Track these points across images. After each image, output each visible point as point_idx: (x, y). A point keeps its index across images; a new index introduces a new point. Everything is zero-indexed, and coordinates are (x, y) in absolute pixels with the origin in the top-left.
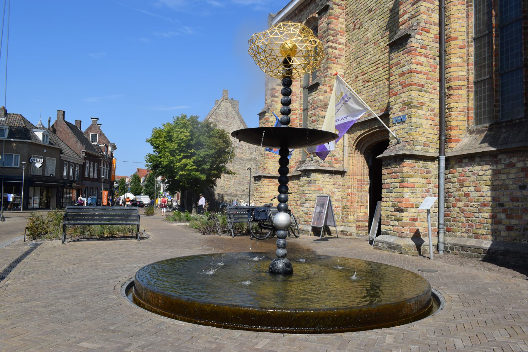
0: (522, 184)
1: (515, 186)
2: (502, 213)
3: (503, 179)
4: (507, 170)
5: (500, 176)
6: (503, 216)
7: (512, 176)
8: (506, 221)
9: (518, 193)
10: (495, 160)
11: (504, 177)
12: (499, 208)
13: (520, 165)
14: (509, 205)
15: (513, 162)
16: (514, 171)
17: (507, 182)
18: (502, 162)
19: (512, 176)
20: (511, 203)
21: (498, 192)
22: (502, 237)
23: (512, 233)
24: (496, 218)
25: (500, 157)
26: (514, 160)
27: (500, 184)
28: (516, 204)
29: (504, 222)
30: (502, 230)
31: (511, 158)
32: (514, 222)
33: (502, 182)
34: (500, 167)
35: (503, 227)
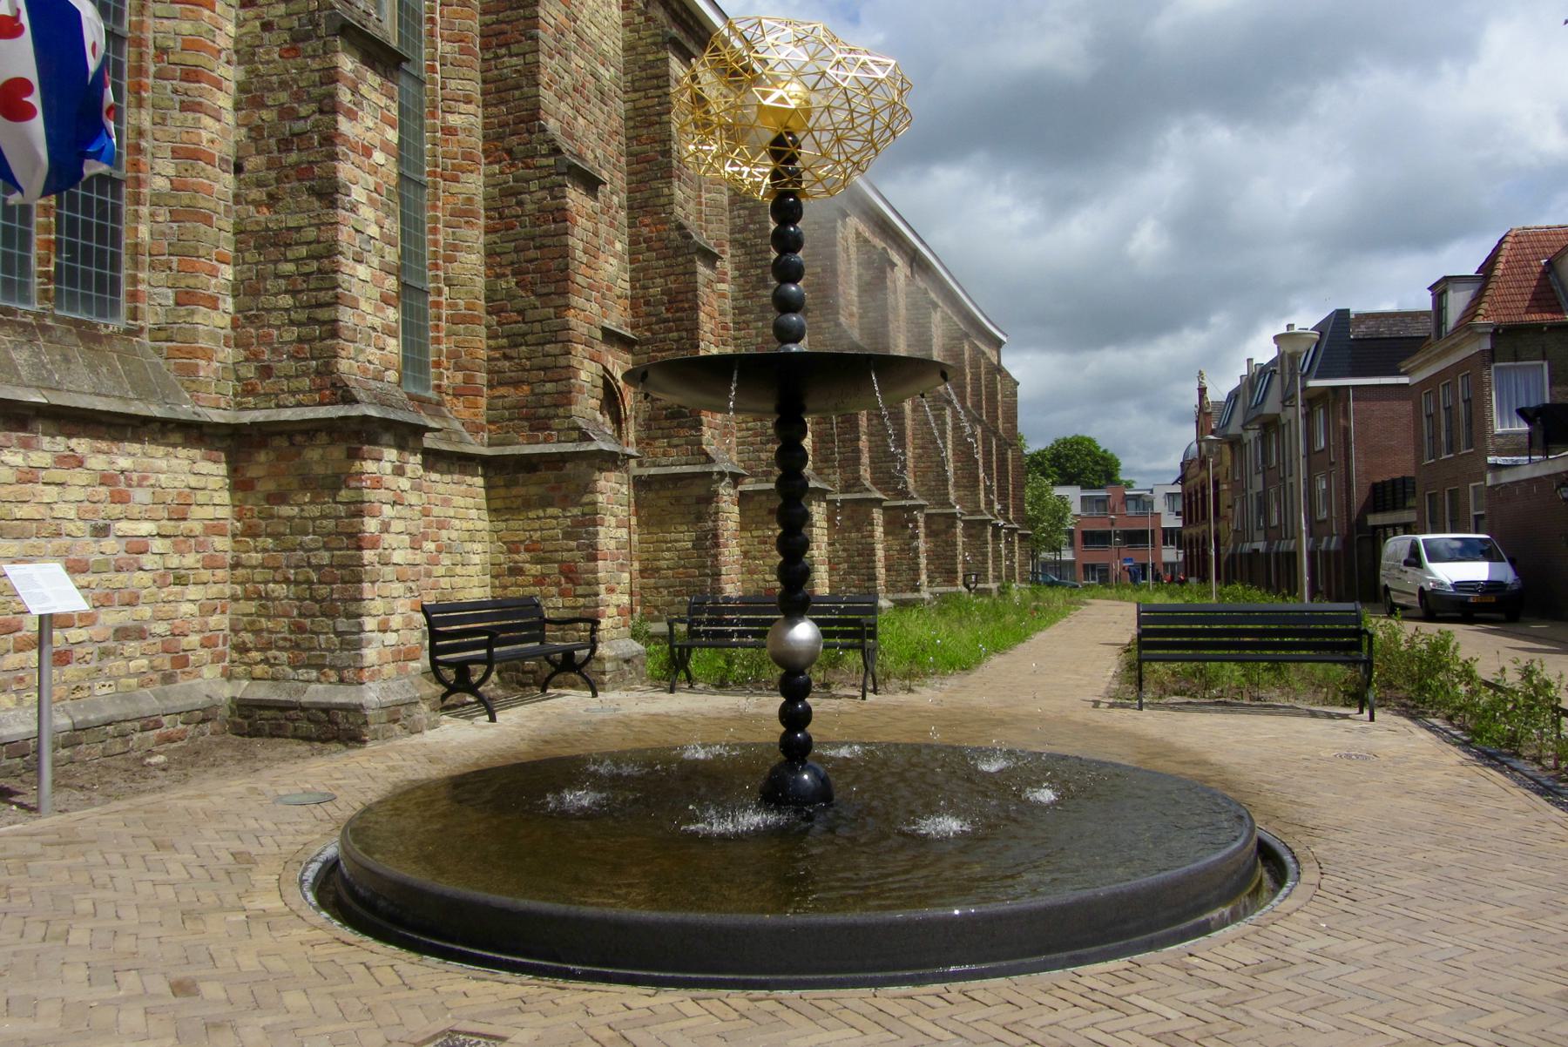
0: (101, 523)
1: (80, 523)
4: (58, 475)
7: (75, 493)
11: (51, 493)
13: (97, 463)
16: (78, 477)
17: (62, 510)
19: (75, 493)
24: (19, 630)
26: (81, 445)
33: (43, 509)
34: (37, 458)
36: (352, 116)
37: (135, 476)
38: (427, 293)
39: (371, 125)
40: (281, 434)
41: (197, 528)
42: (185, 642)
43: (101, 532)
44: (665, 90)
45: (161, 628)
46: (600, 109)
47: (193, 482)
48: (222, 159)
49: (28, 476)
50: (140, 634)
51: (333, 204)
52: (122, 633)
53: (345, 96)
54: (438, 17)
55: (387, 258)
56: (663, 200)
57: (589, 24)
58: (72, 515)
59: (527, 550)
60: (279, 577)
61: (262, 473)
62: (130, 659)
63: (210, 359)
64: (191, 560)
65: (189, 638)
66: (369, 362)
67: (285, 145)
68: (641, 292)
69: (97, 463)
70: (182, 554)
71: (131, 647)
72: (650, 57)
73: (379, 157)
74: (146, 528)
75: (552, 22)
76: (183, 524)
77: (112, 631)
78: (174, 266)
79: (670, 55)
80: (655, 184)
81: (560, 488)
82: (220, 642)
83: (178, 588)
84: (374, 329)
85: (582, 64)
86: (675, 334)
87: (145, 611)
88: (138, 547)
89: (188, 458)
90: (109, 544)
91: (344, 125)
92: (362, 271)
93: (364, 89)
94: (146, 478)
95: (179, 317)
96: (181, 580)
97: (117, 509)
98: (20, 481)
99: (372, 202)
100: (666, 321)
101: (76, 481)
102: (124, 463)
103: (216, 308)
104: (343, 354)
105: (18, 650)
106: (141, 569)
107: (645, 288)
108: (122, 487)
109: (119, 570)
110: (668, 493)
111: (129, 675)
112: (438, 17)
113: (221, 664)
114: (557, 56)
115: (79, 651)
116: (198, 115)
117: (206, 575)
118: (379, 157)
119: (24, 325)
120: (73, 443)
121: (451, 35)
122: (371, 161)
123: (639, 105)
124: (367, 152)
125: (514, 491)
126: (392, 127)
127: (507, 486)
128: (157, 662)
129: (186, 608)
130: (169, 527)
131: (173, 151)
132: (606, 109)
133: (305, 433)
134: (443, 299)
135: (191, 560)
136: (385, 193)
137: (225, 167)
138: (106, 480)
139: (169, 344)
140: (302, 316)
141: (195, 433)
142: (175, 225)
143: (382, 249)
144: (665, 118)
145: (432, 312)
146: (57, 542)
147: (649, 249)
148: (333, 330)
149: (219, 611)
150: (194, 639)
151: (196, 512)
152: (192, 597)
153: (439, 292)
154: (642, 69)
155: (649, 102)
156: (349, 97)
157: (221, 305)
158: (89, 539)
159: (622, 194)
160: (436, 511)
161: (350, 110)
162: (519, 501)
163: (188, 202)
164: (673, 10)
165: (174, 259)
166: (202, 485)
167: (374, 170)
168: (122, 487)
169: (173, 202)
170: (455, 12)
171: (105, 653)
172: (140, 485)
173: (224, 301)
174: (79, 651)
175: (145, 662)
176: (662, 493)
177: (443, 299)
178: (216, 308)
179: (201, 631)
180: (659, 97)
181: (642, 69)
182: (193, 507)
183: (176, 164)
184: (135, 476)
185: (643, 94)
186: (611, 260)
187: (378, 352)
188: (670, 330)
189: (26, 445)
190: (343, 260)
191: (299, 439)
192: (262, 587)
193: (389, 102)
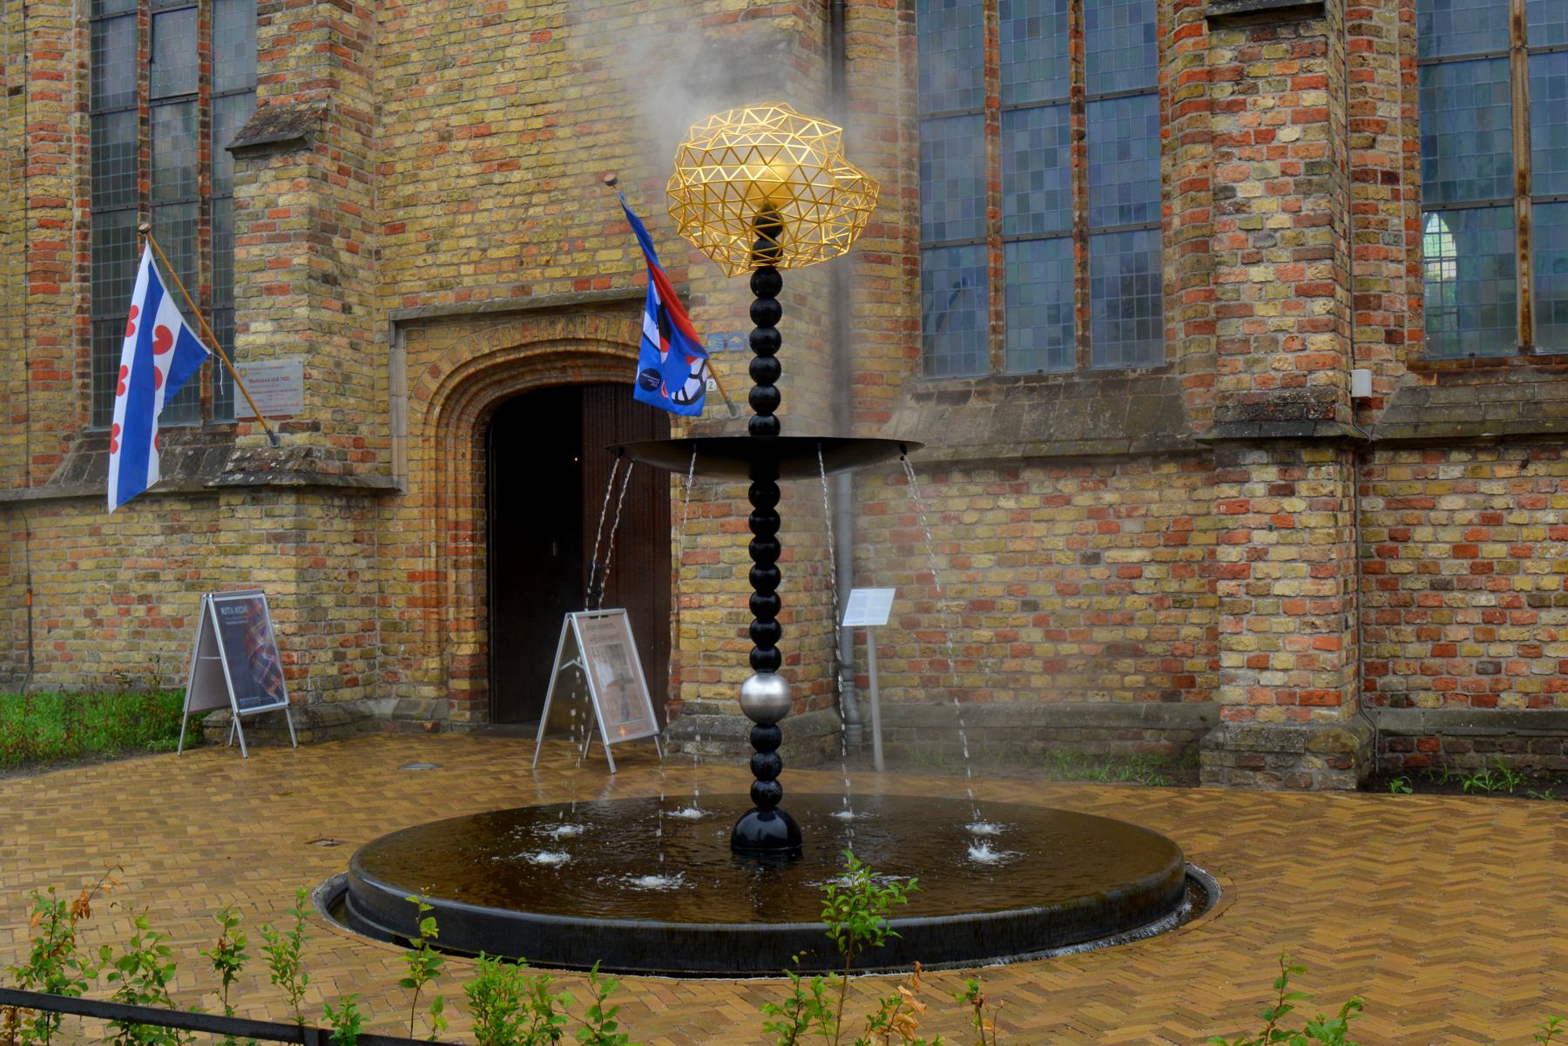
0: (1089, 552)
2: (1034, 625)
3: (1036, 534)
4: (1047, 512)
5: (1028, 525)
6: (1036, 635)
7: (1062, 528)
8: (1047, 649)
9: (1081, 575)
10: (1013, 483)
11: (1040, 530)
12: (1025, 614)
13: (1084, 500)
14: (1052, 602)
15: (1066, 491)
16: (1067, 514)
17: (1050, 543)
18: (1035, 489)
19: (1062, 528)
20: (1059, 600)
21: (1021, 569)
22: (1032, 690)
23: (1062, 680)
24: (1015, 640)
25: (1027, 475)
26: (1068, 486)
27: (1028, 548)
28: (1071, 602)
29: (1038, 650)
30: (1033, 673)
31: (1058, 479)
32: (1066, 648)
33: (1033, 543)
34: (1027, 501)
35: (1038, 664)
37: (1123, 510)
42: (1188, 665)
43: (1092, 559)
45: (1158, 648)
47: (1191, 509)
49: (1021, 516)
50: (1136, 651)
52: (1116, 650)
58: (1061, 545)
62: (1126, 674)
69: (1084, 500)
70: (1182, 579)
71: (1126, 663)
73: (1287, 134)
74: (1137, 555)
76: (1181, 551)
77: (1102, 647)
83: (1179, 612)
87: (1142, 633)
88: (1132, 573)
89: (1185, 486)
90: (1098, 572)
94: (1135, 509)
96: (1179, 603)
97: (1105, 539)
98: (1013, 521)
101: (1063, 517)
102: (1109, 497)
105: (1014, 657)
106: (1134, 593)
108: (1112, 519)
109: (1110, 593)
111: (1123, 688)
115: (1071, 663)
119: (1050, 388)
120: (1061, 485)
124: (1266, 136)
128: (1156, 679)
129: (1186, 631)
130: (1164, 553)
138: (1093, 513)
141: (1193, 461)
146: (1047, 570)
151: (1197, 538)
158: (1079, 566)
166: (1203, 510)
168: (1112, 519)
171: (1098, 666)
172: (1129, 516)
174: (1071, 663)
175: (1140, 678)
184: (1123, 510)
189: (1018, 491)
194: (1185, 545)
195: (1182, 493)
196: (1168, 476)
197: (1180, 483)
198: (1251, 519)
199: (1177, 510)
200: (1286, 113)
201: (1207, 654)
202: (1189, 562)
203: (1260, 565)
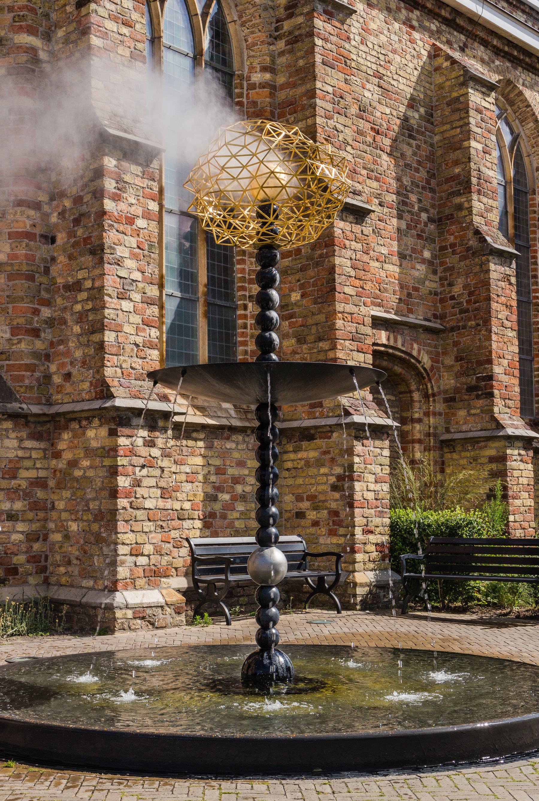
36: (116, 198)
38: (235, 309)
39: (134, 201)
40: (74, 419)
41: (24, 484)
44: (466, 120)
46: (409, 144)
47: (20, 453)
48: (42, 236)
51: (101, 262)
53: (110, 185)
54: (245, 100)
55: (149, 294)
56: (464, 213)
57: (396, 77)
59: (307, 500)
60: (73, 517)
61: (65, 447)
63: (34, 371)
64: (18, 505)
65: (19, 557)
66: (132, 368)
67: (77, 221)
68: (447, 289)
72: (455, 94)
75: (330, 89)
78: (10, 311)
79: (470, 90)
80: (457, 200)
81: (328, 452)
82: (43, 559)
84: (137, 345)
85: (388, 111)
86: (473, 323)
91: (109, 205)
92: (126, 305)
93: (127, 178)
95: (13, 345)
99: (134, 256)
100: (467, 311)
103: (38, 336)
104: (108, 364)
107: (451, 285)
110: (468, 454)
112: (245, 100)
113: (42, 575)
114: (336, 115)
116: (24, 208)
117: (30, 515)
118: (141, 223)
121: (254, 112)
122: (134, 227)
123: (447, 135)
125: (300, 455)
126: (154, 200)
127: (295, 451)
131: (9, 234)
132: (414, 143)
133: (87, 419)
134: (248, 312)
135: (18, 505)
136: (146, 247)
137: (43, 241)
139: (7, 362)
140: (84, 339)
142: (10, 283)
143: (143, 288)
144: (466, 144)
145: (240, 322)
147: (454, 253)
148: (101, 346)
149: (41, 539)
150: (21, 558)
151: (24, 474)
152: (21, 530)
153: (245, 307)
154: (449, 104)
155: (453, 132)
156: (114, 185)
157: (43, 335)
159: (432, 211)
160: (230, 471)
161: (115, 194)
162: (303, 462)
163: (17, 268)
164: (494, 47)
165: (10, 306)
166: (27, 455)
167: (137, 232)
169: (9, 268)
170: (257, 93)
173: (45, 332)
176: (463, 454)
177: (248, 312)
178: (38, 336)
179: (26, 552)
180: (461, 127)
181: (449, 104)
182: (20, 471)
183: (11, 244)
185: (448, 127)
186: (418, 266)
187: (140, 361)
188: (470, 319)
190: (110, 300)
191: (84, 423)
192: (65, 524)
193: (151, 183)
194: (15, 478)
195: (15, 443)
196: (7, 430)
197: (13, 435)
198: (136, 460)
199: (11, 454)
200: (140, 212)
201: (26, 552)
202: (16, 490)
203: (138, 489)
